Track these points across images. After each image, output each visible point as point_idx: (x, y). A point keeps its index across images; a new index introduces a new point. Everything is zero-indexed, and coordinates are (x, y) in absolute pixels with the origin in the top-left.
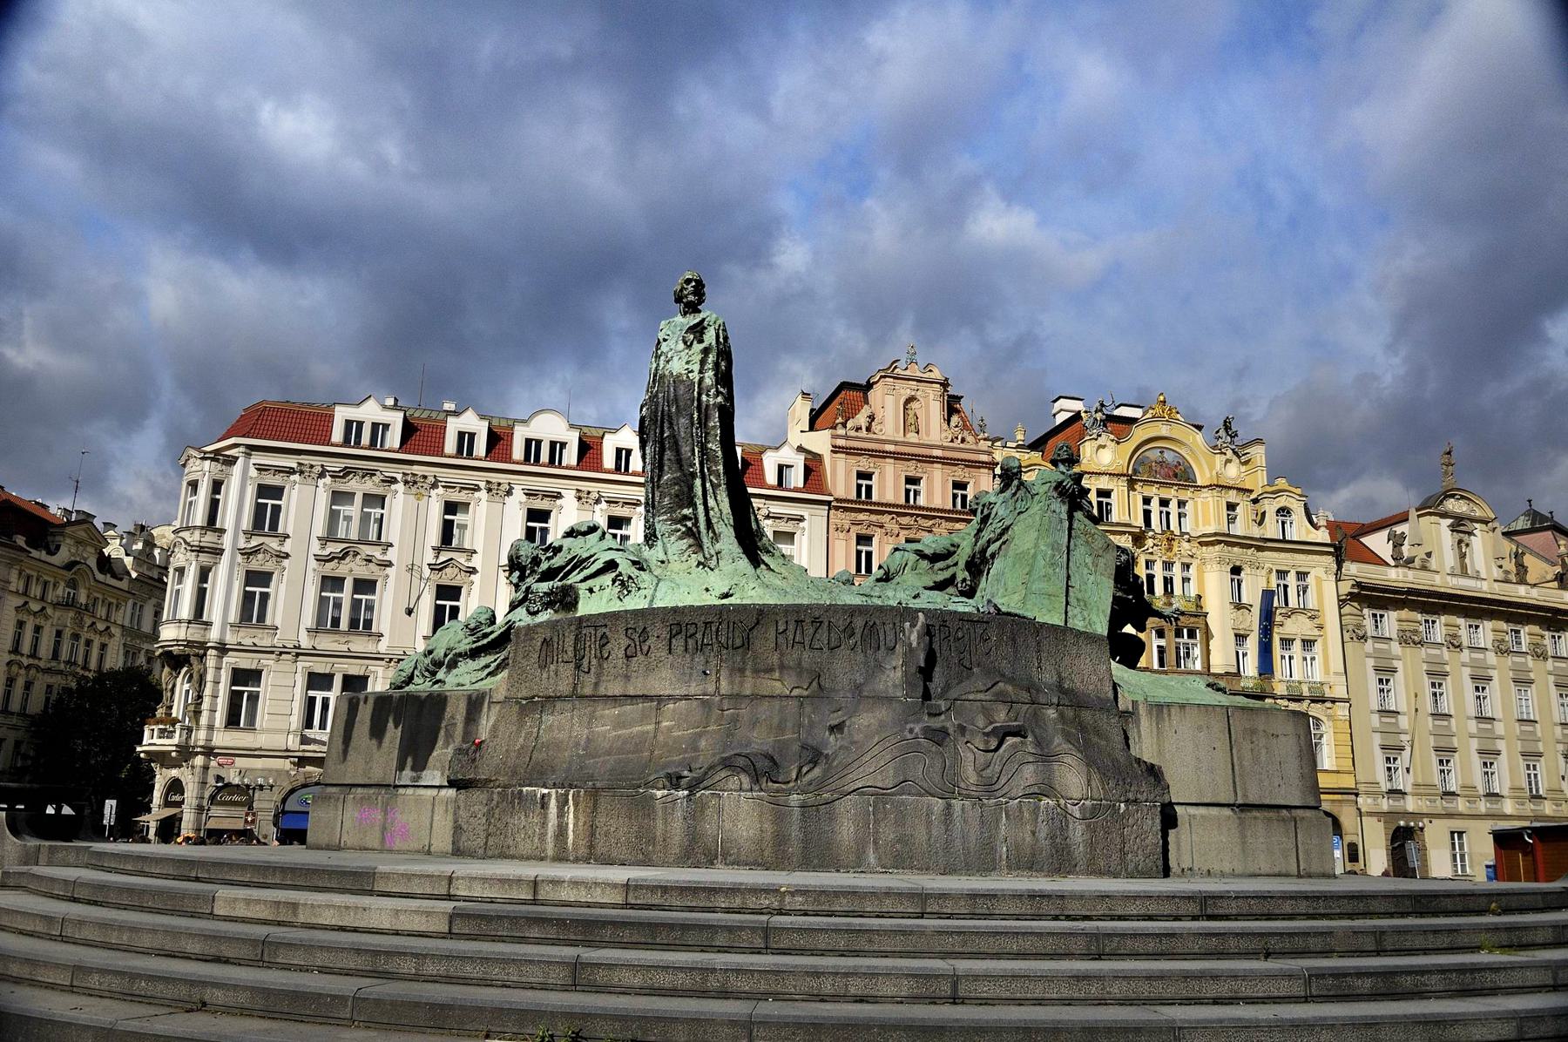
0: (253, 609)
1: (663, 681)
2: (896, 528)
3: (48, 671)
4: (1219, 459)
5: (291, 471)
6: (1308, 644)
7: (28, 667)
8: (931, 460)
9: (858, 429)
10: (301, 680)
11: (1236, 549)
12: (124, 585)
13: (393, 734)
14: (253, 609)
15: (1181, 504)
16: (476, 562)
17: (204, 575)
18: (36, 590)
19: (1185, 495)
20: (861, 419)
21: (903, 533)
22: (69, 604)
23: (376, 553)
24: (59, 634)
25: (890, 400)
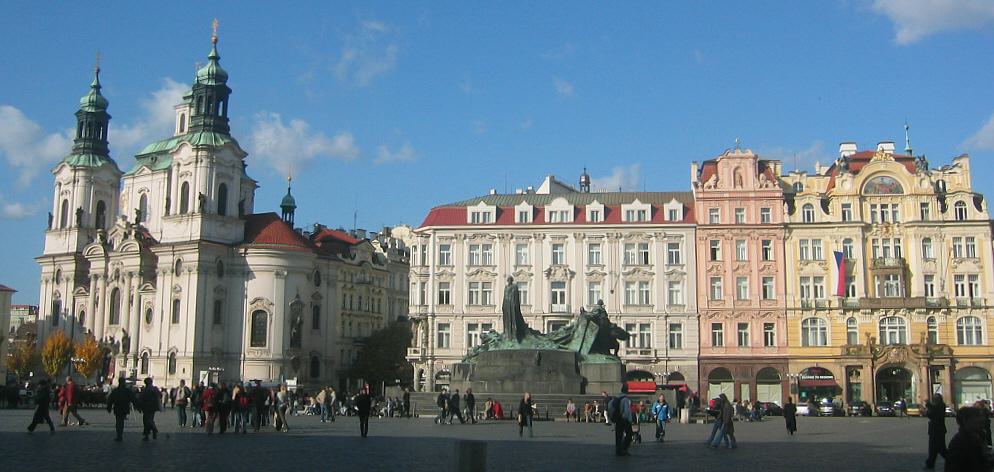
0: (444, 298)
1: (499, 364)
2: (731, 236)
3: (356, 316)
4: (916, 180)
5: (452, 238)
6: (973, 277)
7: (350, 315)
8: (748, 199)
9: (710, 187)
10: (465, 327)
11: (926, 228)
12: (385, 268)
13: (462, 372)
14: (444, 298)
15: (894, 206)
16: (533, 270)
17: (423, 284)
18: (348, 278)
19: (897, 201)
20: (711, 182)
21: (735, 238)
22: (361, 283)
23: (490, 270)
24: (360, 298)
25: (726, 170)
